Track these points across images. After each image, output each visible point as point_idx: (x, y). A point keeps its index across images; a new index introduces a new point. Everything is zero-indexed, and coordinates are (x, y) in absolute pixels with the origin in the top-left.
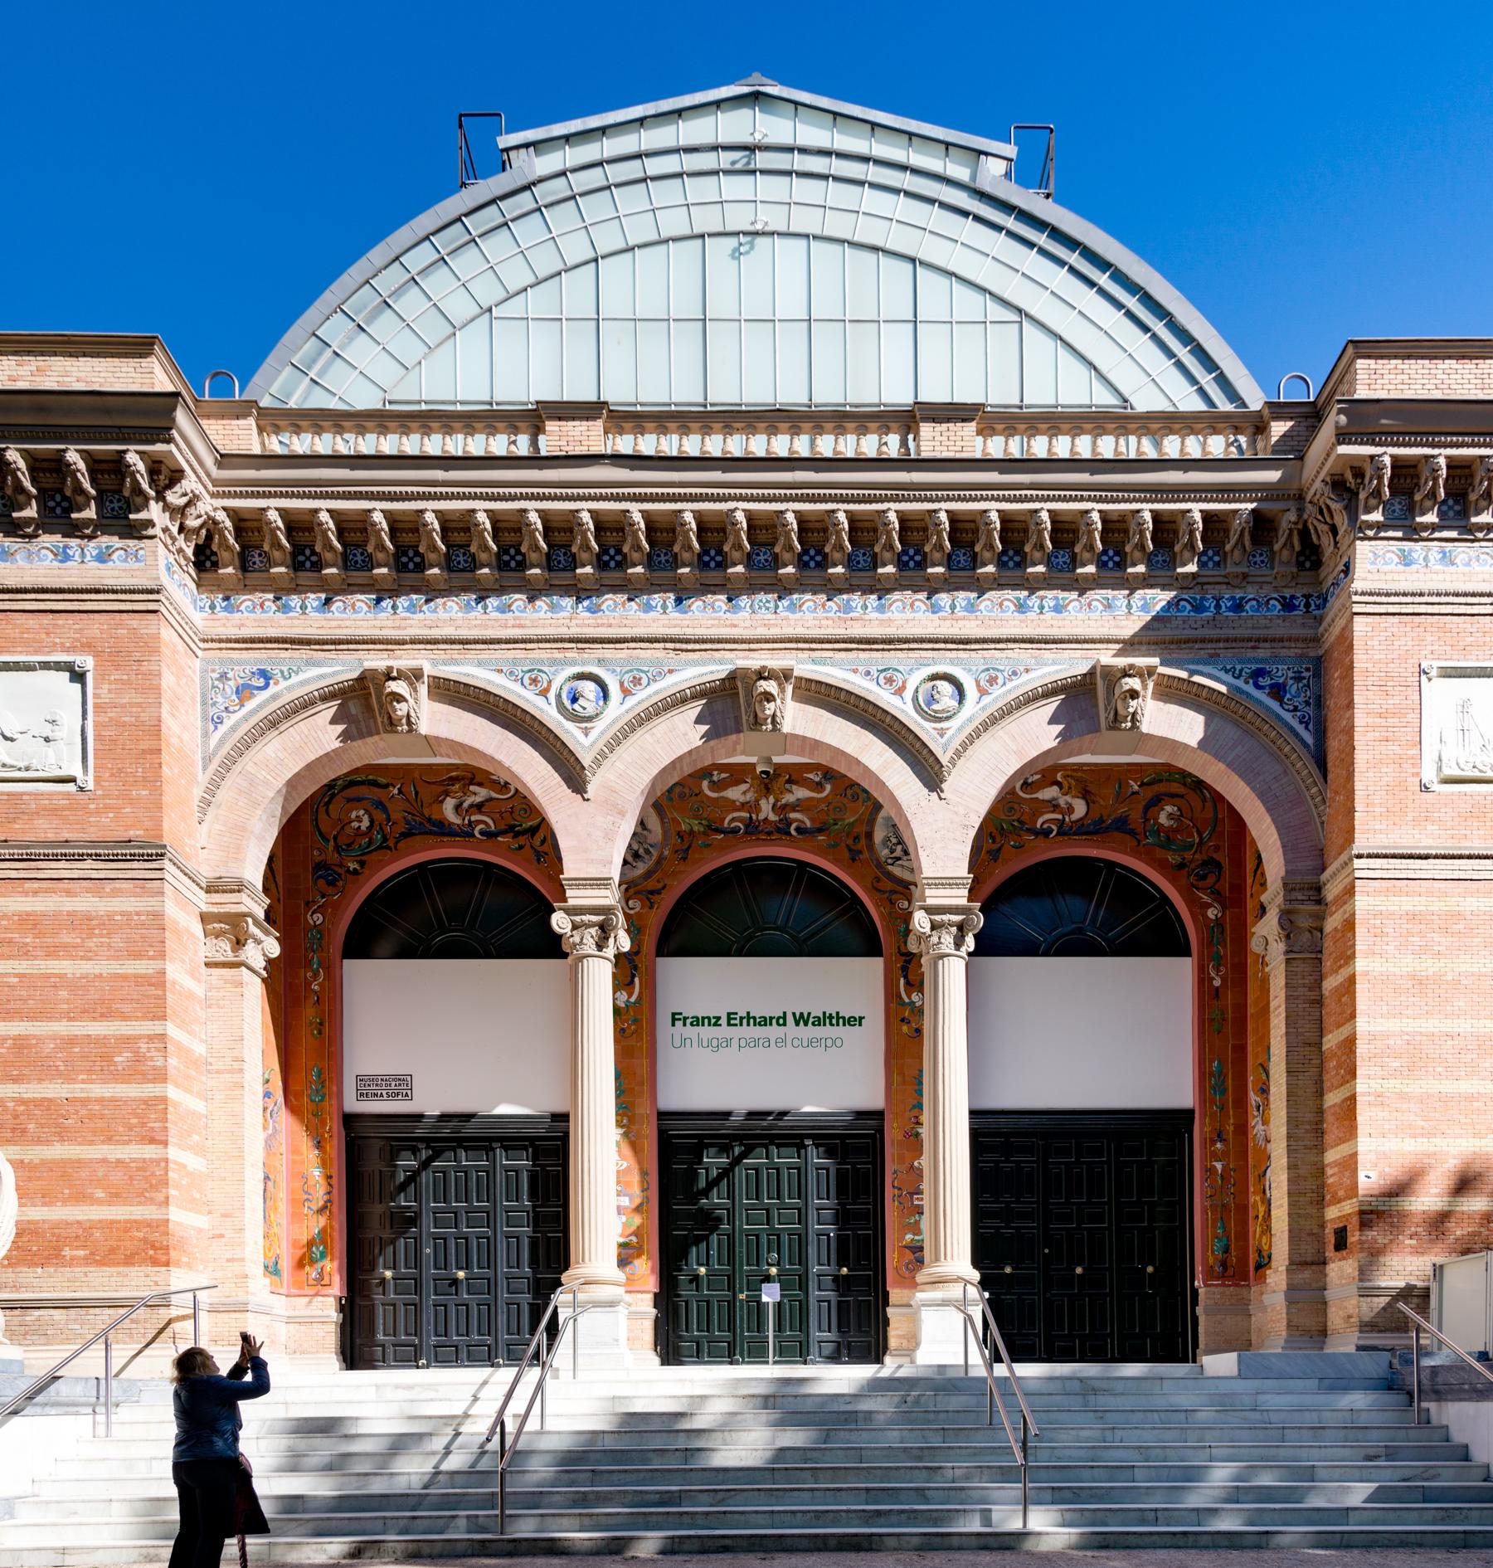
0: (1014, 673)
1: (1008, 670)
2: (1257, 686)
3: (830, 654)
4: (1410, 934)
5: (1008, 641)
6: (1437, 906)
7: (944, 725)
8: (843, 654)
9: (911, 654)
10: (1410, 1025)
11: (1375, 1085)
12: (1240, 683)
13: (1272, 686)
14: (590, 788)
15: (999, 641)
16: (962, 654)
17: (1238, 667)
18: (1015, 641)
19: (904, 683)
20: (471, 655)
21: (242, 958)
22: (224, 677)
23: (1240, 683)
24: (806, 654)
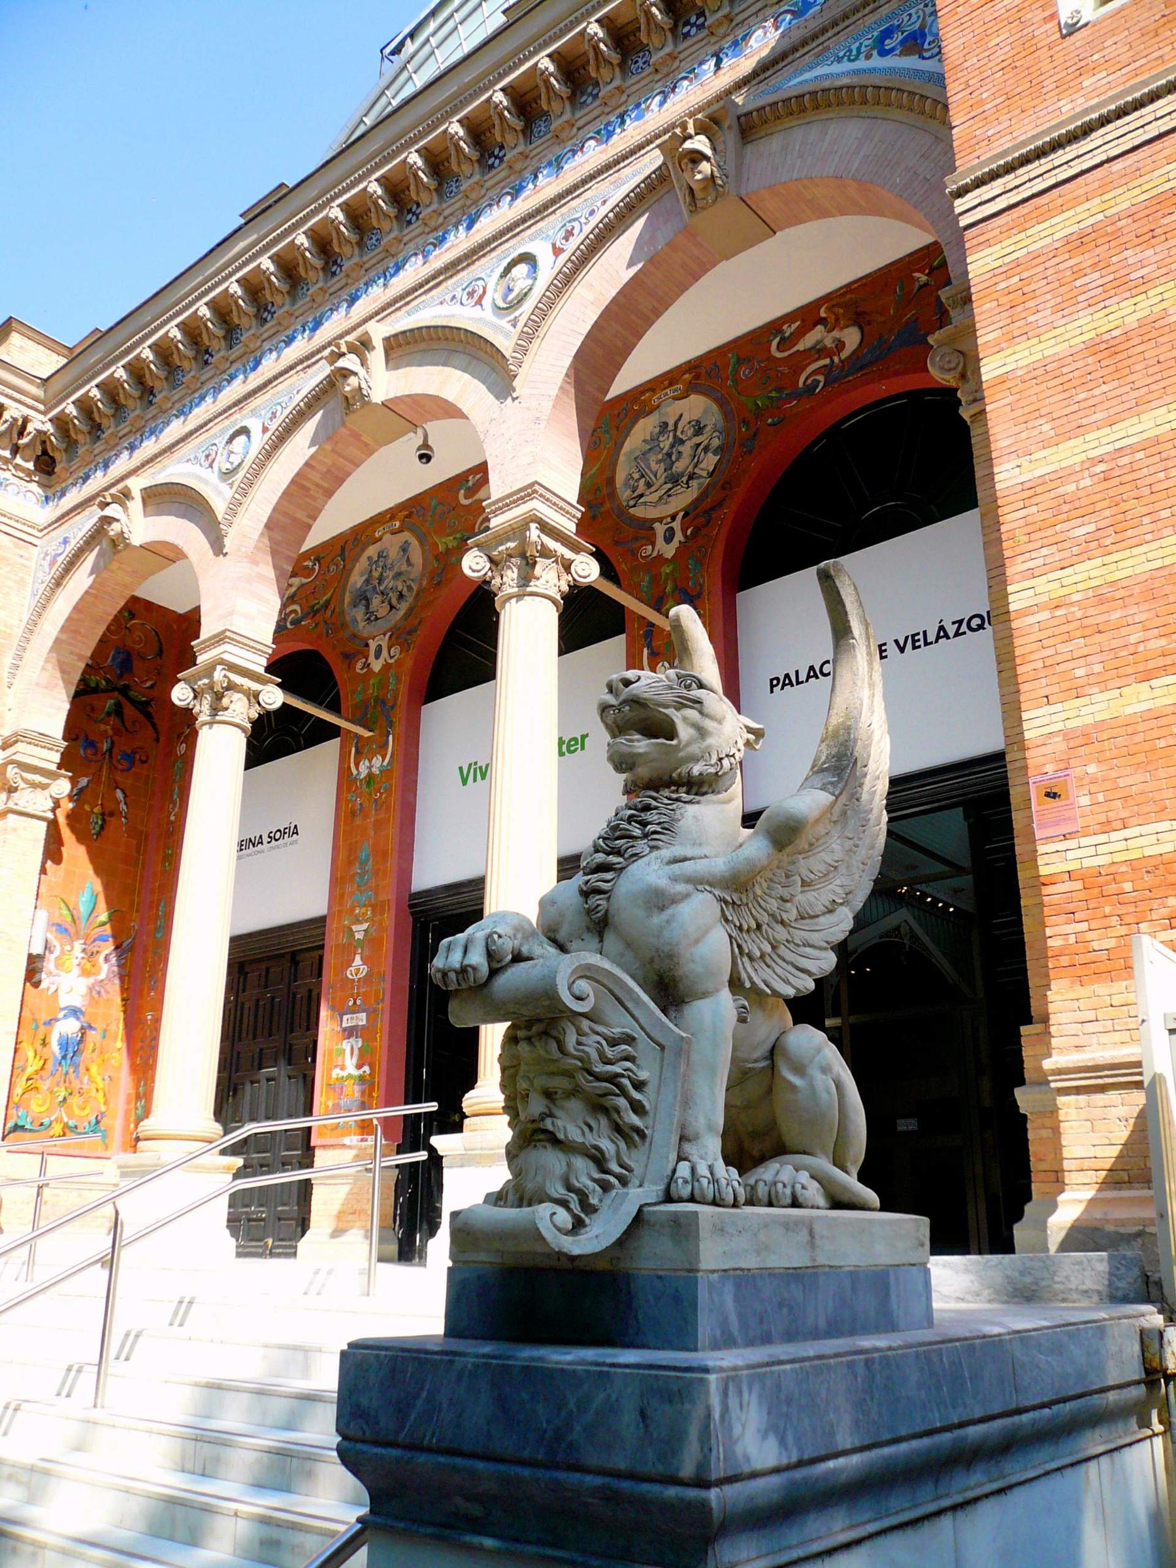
0: (592, 213)
1: (586, 212)
2: (883, 53)
3: (423, 298)
4: (1078, 273)
5: (584, 182)
6: (1123, 200)
7: (517, 314)
8: (434, 292)
9: (494, 254)
10: (1100, 442)
11: (1046, 587)
12: (861, 64)
13: (903, 42)
14: (227, 541)
15: (575, 187)
16: (541, 225)
17: (854, 47)
18: (592, 177)
19: (484, 289)
20: (176, 456)
21: (11, 805)
22: (46, 554)
23: (861, 64)
24: (399, 314)
